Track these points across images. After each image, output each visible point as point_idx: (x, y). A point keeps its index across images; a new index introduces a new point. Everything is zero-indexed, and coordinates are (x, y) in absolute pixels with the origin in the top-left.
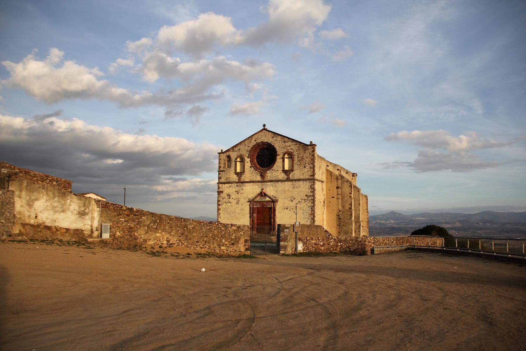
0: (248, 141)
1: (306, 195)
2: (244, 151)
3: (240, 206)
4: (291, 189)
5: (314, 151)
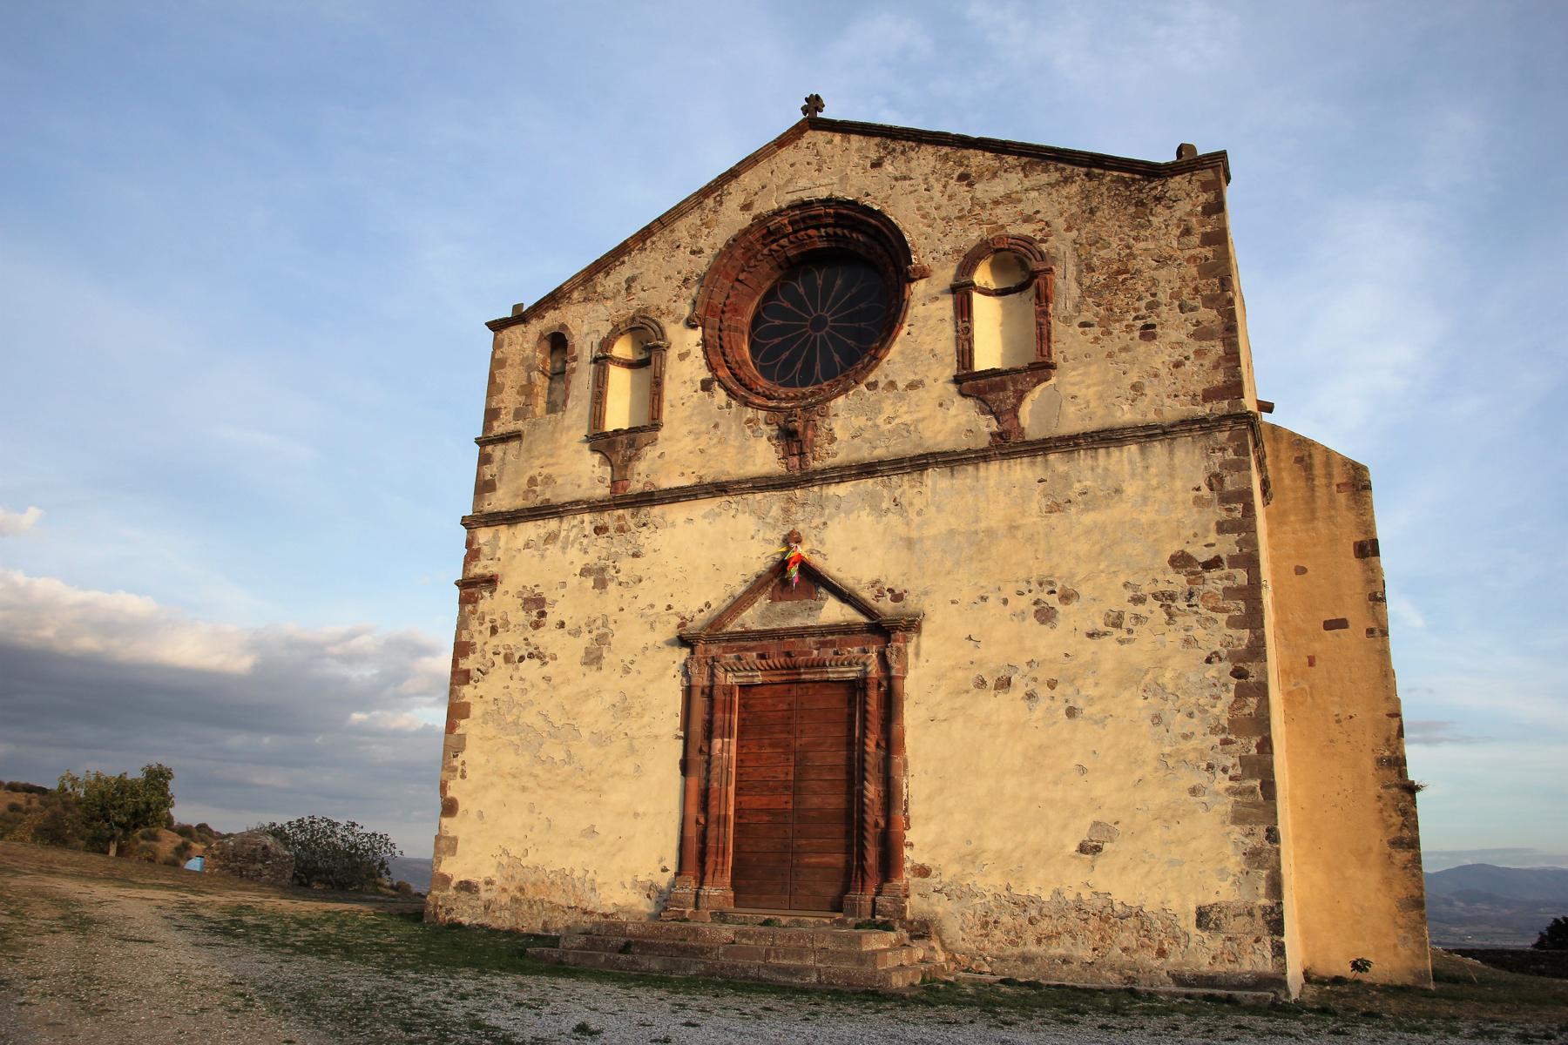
0: (694, 218)
1: (1180, 561)
2: (665, 284)
3: (609, 680)
4: (1033, 518)
5: (1216, 207)
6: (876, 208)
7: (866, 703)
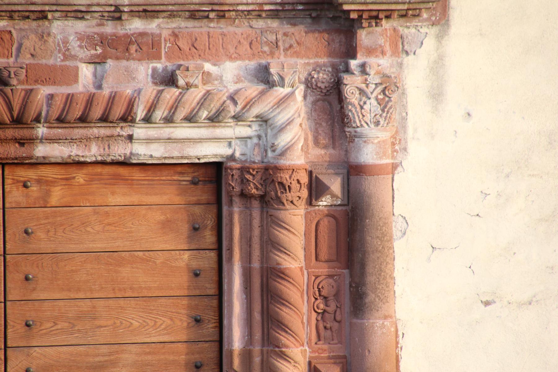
7: (271, 244)
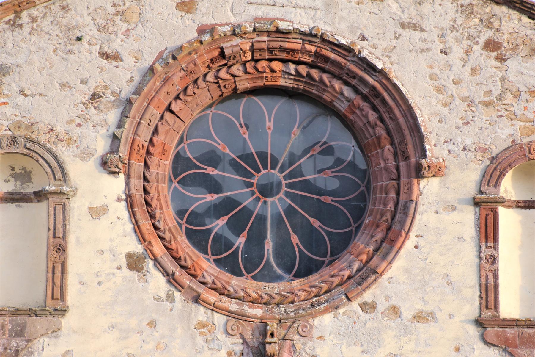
6: (379, 66)
